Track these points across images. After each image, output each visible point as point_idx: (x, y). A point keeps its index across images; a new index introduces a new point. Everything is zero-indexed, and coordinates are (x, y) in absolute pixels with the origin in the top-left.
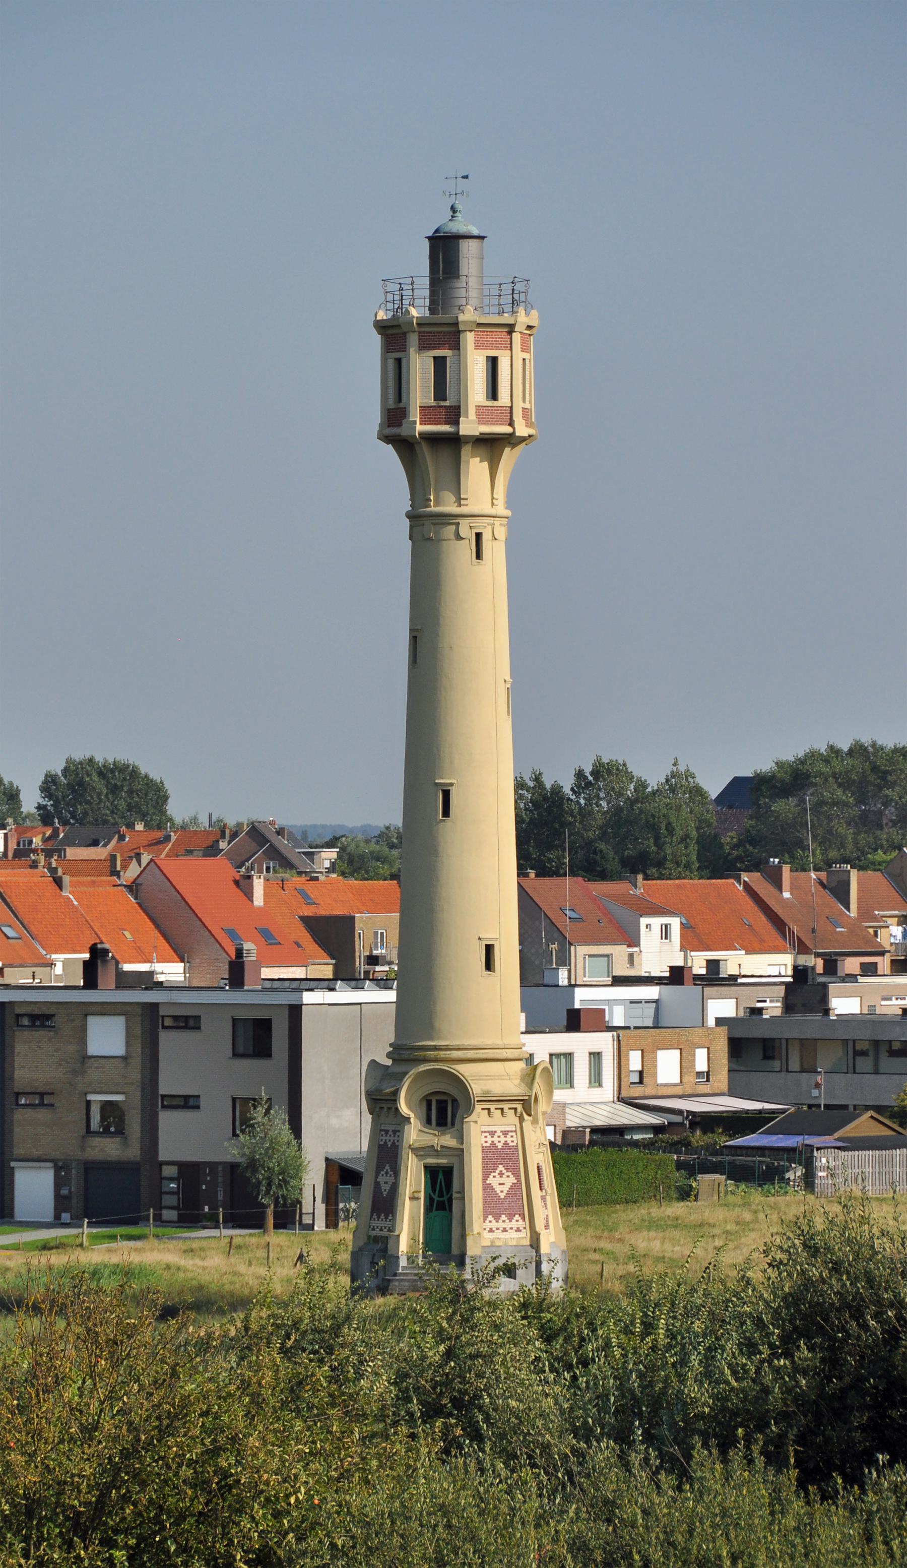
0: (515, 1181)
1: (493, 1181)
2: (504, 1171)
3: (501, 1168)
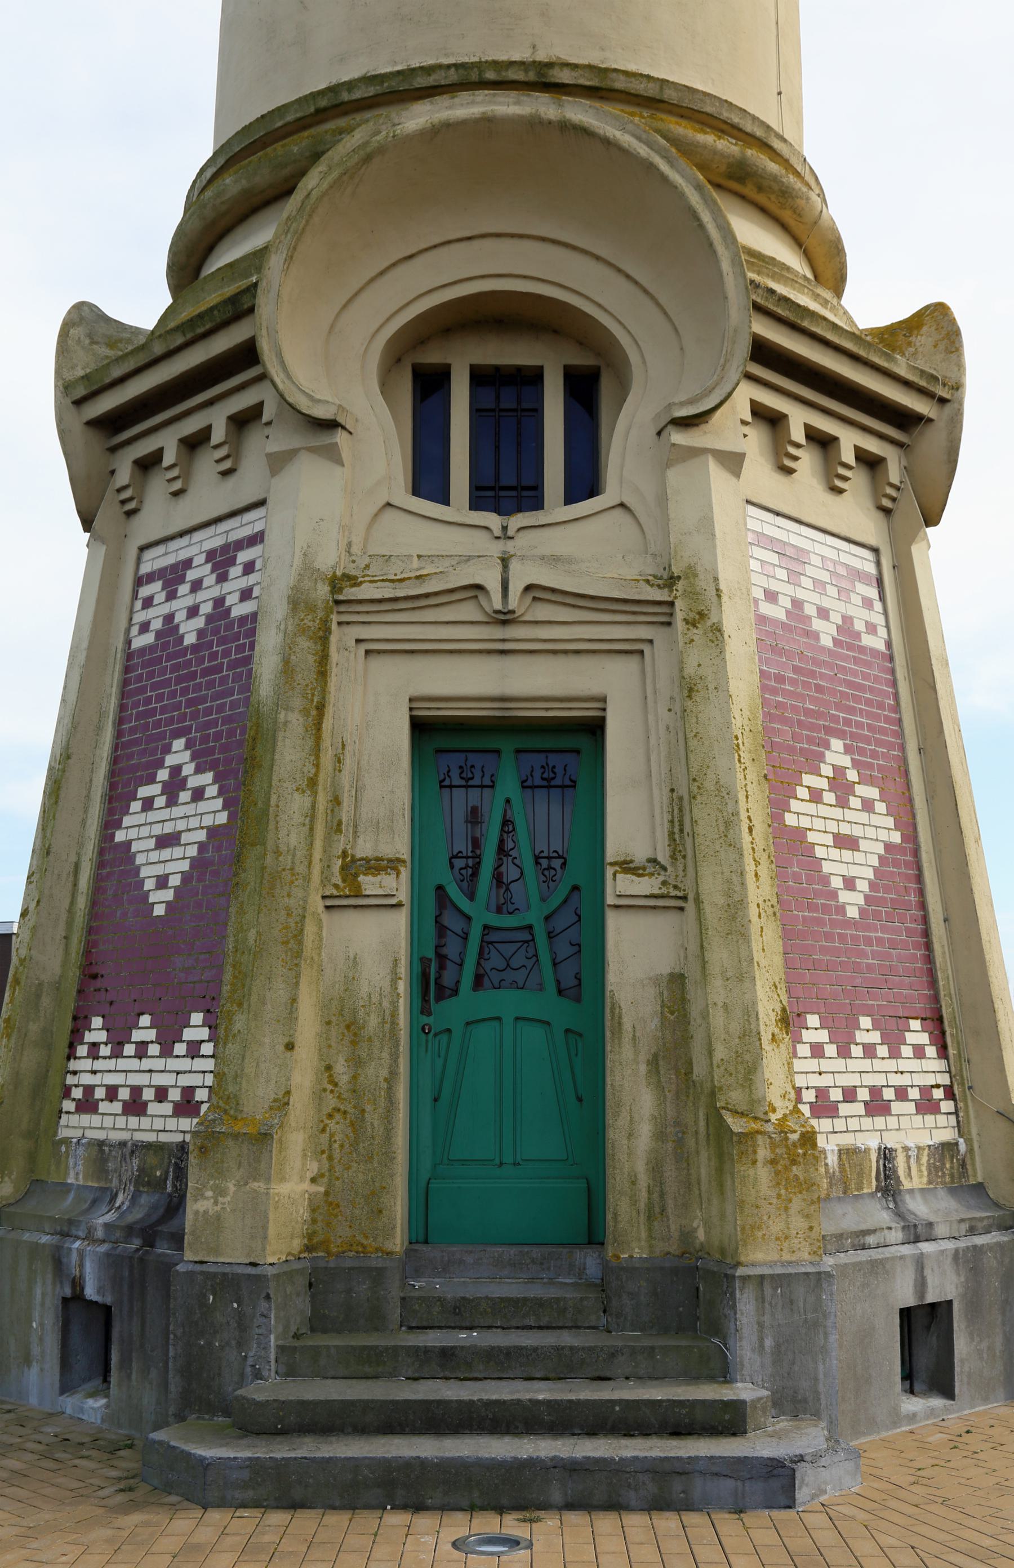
0: (896, 838)
1: (811, 816)
2: (852, 775)
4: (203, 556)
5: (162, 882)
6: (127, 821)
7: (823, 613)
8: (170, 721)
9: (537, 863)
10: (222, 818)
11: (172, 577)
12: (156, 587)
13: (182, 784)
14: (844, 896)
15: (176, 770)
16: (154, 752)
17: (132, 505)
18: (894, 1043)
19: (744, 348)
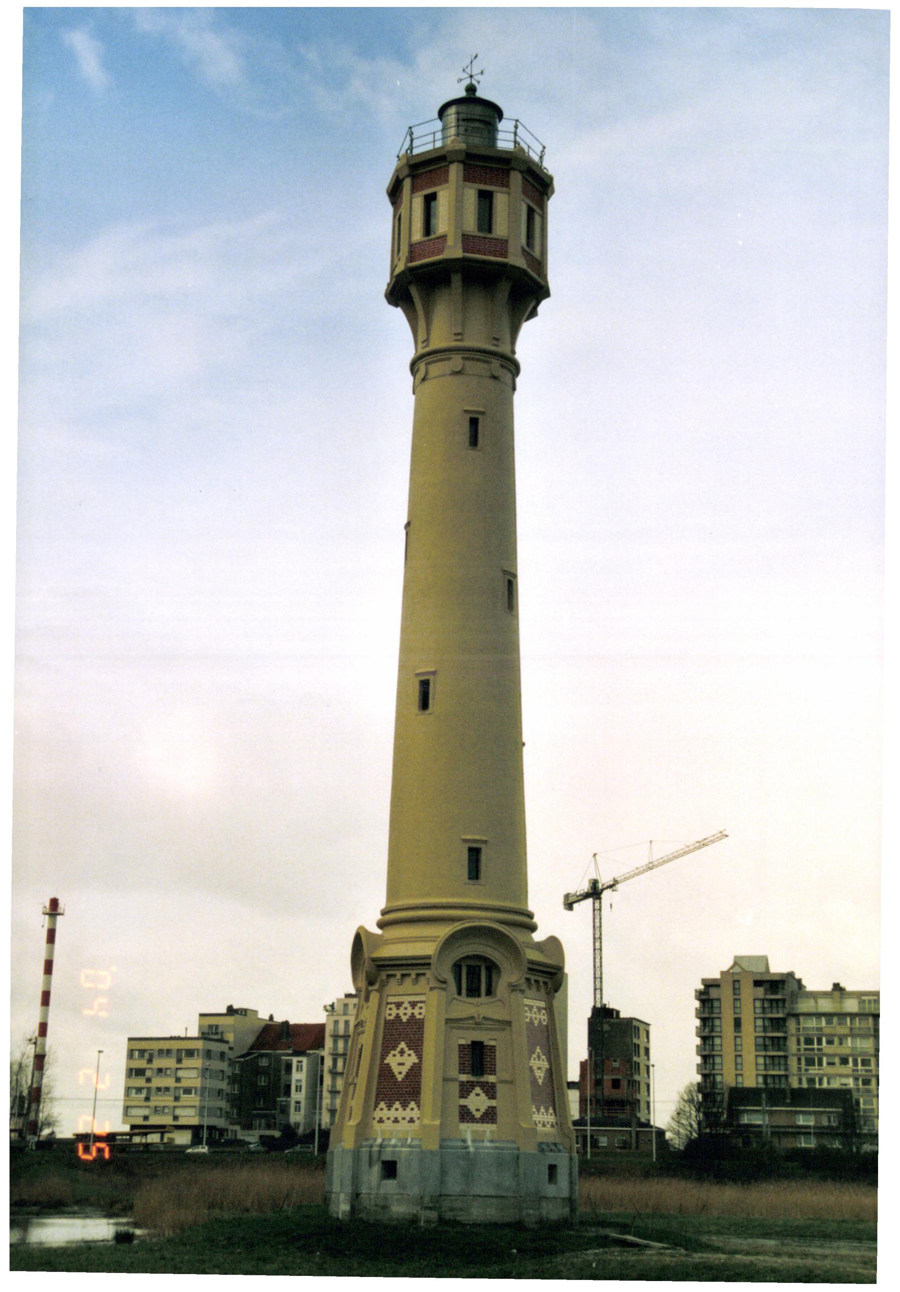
10: (417, 1061)
11: (399, 1005)
12: (393, 1006)
15: (402, 1049)
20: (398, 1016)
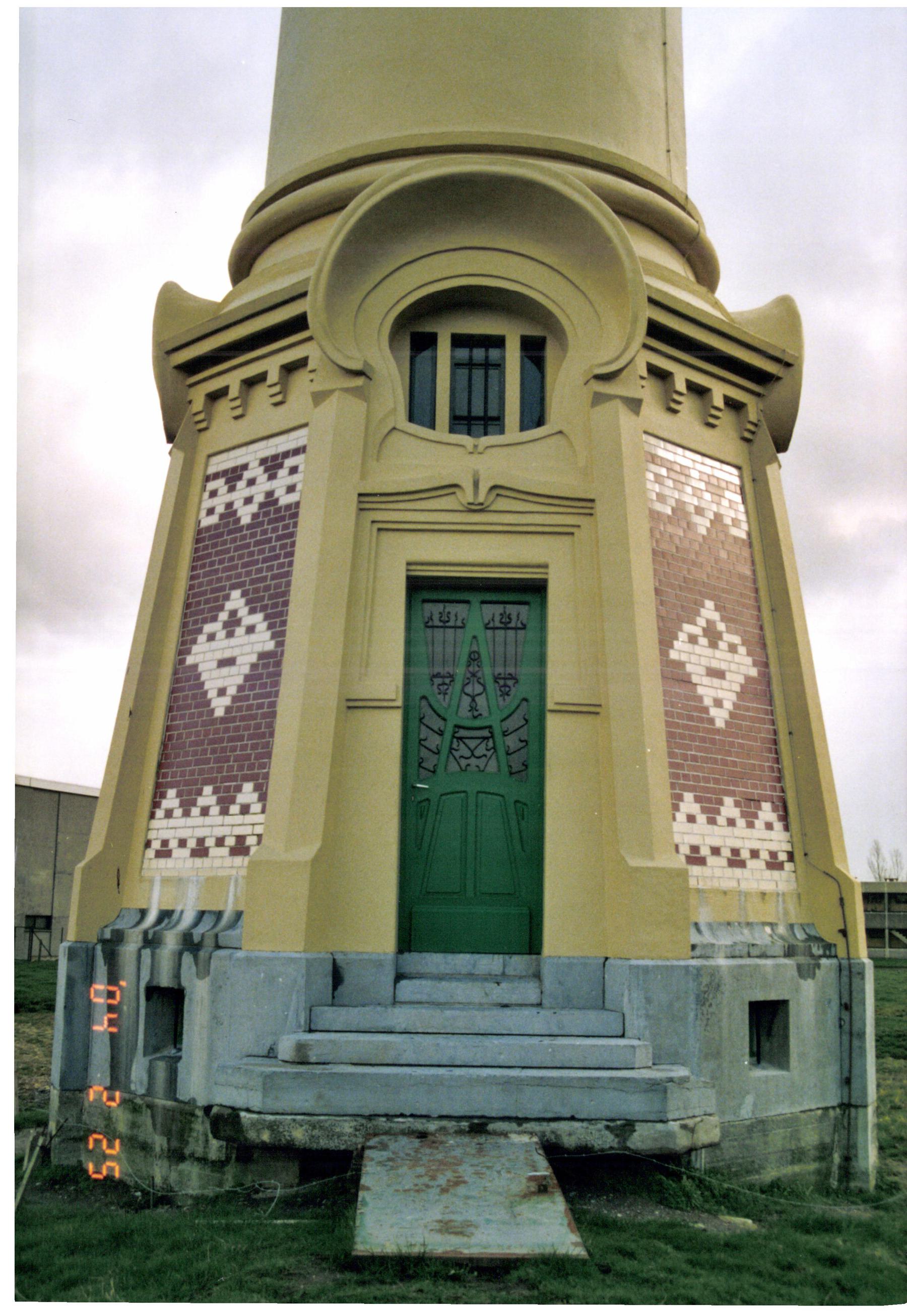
2: (721, 627)
3: (709, 611)
4: (257, 462)
5: (222, 692)
6: (195, 649)
7: (699, 511)
8: (229, 578)
9: (496, 682)
10: (270, 646)
11: (233, 476)
13: (238, 622)
14: (713, 712)
16: (216, 599)
17: (203, 425)
18: (750, 819)
19: (643, 327)
20: (230, 511)
